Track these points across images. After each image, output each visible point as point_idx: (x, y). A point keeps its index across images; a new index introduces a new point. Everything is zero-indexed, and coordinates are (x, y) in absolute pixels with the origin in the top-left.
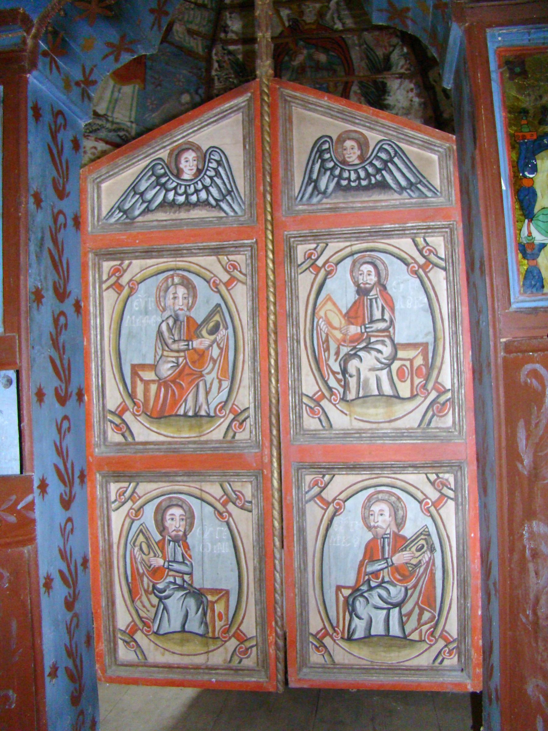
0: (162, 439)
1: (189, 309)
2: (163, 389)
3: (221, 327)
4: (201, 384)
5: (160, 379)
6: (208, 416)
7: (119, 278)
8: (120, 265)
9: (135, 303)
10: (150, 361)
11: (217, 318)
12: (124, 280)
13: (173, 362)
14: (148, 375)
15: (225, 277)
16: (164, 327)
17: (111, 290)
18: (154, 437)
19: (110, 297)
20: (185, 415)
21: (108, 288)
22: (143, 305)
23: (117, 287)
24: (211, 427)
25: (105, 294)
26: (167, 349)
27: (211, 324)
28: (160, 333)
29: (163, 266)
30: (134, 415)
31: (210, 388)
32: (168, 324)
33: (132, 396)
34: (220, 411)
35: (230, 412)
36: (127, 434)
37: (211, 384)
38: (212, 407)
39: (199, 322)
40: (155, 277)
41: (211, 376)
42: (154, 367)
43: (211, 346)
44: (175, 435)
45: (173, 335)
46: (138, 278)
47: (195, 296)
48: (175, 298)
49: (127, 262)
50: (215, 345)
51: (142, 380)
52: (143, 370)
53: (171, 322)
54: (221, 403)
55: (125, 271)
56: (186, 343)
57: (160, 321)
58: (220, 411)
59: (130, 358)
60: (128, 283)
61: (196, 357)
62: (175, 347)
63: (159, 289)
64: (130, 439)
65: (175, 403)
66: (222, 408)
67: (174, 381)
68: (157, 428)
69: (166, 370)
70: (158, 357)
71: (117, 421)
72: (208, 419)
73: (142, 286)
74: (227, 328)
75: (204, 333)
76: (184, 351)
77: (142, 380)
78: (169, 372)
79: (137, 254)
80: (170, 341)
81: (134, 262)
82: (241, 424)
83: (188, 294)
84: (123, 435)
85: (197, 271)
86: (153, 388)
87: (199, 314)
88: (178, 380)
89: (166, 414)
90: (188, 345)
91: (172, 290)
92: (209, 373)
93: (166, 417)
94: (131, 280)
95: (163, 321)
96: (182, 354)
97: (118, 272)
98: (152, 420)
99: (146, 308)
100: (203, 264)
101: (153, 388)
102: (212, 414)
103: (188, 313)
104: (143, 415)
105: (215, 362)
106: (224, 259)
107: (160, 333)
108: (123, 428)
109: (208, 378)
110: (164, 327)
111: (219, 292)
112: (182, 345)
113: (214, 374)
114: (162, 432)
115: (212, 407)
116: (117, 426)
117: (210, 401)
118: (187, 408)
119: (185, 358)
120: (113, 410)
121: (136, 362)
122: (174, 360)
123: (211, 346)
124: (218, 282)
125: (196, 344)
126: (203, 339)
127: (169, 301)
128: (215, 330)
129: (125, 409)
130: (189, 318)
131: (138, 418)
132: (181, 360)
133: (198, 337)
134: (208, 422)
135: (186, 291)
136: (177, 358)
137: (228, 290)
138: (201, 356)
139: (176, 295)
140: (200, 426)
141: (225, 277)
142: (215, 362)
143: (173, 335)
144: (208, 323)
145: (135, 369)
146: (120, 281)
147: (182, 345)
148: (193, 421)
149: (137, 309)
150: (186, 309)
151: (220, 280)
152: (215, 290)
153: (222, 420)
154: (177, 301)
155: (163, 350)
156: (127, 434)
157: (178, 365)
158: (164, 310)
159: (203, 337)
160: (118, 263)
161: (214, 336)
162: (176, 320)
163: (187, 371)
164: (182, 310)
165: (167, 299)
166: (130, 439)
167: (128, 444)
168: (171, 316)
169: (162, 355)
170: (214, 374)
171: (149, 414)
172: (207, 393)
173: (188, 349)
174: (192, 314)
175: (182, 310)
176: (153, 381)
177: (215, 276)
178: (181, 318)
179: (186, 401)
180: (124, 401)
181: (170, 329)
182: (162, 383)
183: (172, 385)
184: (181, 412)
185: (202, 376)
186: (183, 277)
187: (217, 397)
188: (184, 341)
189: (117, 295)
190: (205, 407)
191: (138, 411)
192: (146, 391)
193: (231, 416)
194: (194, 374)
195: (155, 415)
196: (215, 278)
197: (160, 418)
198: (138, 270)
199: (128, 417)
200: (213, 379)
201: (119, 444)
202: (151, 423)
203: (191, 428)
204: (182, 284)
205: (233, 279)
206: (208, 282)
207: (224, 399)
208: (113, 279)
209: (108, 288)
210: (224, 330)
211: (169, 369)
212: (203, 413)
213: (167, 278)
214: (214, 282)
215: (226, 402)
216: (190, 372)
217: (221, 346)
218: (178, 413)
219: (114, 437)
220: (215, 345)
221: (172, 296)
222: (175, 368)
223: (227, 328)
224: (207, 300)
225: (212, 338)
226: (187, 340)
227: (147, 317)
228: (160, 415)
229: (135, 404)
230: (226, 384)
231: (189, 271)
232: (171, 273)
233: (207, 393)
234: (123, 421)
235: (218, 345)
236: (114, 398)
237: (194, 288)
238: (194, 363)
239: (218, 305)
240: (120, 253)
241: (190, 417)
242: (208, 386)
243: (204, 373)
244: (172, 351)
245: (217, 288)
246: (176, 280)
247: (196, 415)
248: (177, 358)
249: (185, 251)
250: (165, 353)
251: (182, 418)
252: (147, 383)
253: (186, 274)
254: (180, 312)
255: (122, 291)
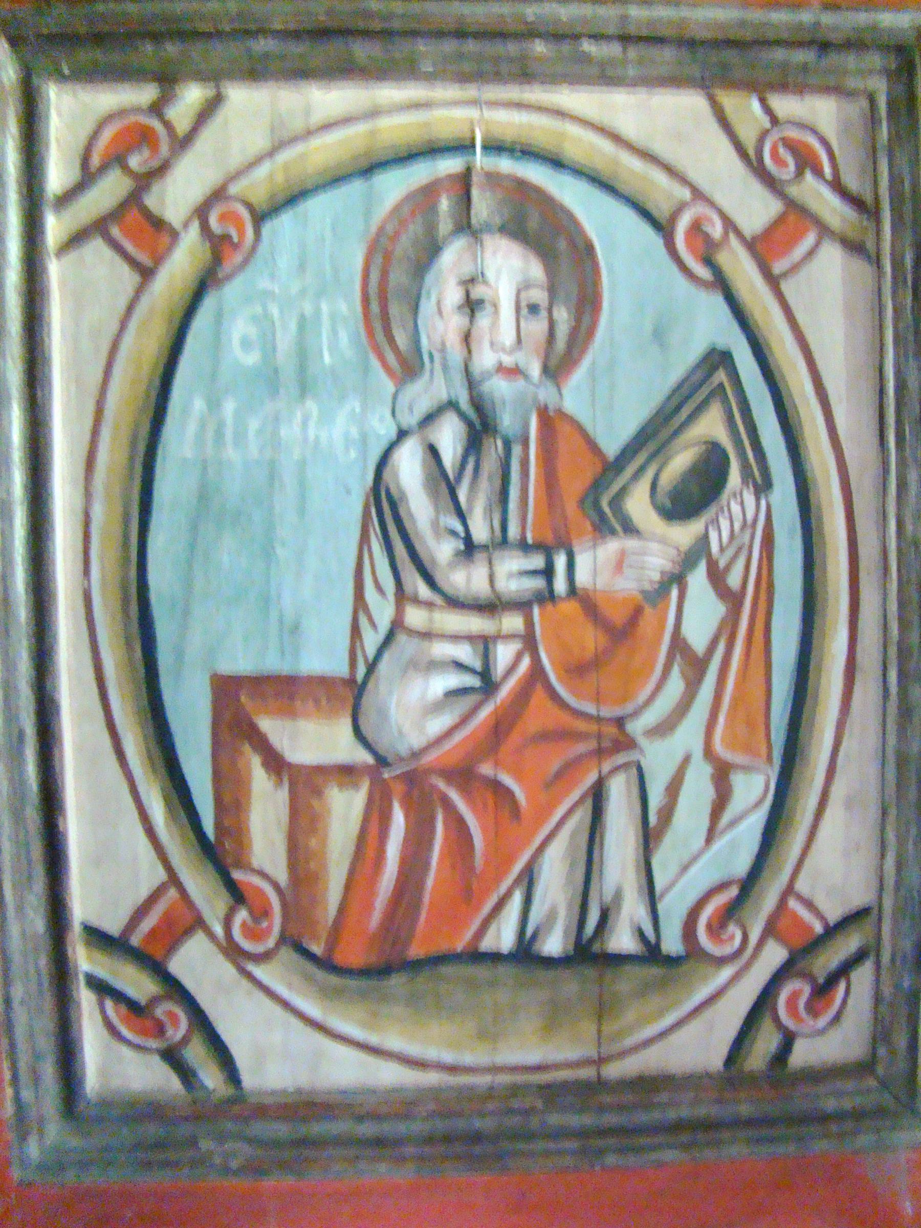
0: (389, 1075)
1: (557, 368)
2: (399, 818)
3: (734, 477)
4: (619, 791)
5: (382, 761)
6: (652, 953)
7: (145, 181)
8: (157, 109)
9: (240, 328)
10: (322, 654)
11: (711, 425)
12: (178, 194)
13: (459, 666)
14: (315, 739)
15: (756, 209)
16: (409, 467)
17: (96, 251)
18: (343, 1070)
19: (85, 290)
20: (525, 953)
21: (76, 240)
22: (285, 342)
23: (136, 231)
24: (661, 1013)
25: (54, 269)
26: (424, 591)
27: (680, 461)
28: (383, 502)
29: (397, 128)
30: (233, 952)
31: (667, 813)
32: (433, 451)
33: (220, 853)
34: (717, 928)
35: (770, 930)
36: (196, 1053)
37: (674, 789)
38: (674, 909)
39: (611, 447)
40: (357, 187)
41: (673, 746)
42: (350, 693)
43: (677, 578)
44: (468, 1059)
45: (461, 516)
46: (258, 185)
47: (588, 303)
48: (471, 306)
49: (192, 95)
50: (698, 579)
51: (275, 763)
52: (290, 713)
53: (449, 437)
54: (722, 887)
55: (183, 143)
56: (537, 561)
57: (385, 430)
58: (717, 928)
59: (206, 645)
60: (202, 212)
61: (590, 639)
62: (470, 580)
63: (379, 250)
64: (211, 1078)
65: (468, 888)
66: (730, 912)
67: (463, 775)
68: (364, 1025)
69: (417, 708)
70: (371, 641)
71: (138, 984)
72: (655, 971)
73: (283, 226)
74: (763, 486)
75: (639, 505)
76: (522, 606)
77: (275, 763)
78: (437, 725)
79: (262, 45)
80: (443, 551)
81: (239, 95)
82: (823, 990)
83: (552, 290)
84: (172, 1057)
85: (600, 165)
86: (345, 808)
87: (611, 398)
88: (486, 769)
89: (416, 951)
90: (548, 572)
91: (453, 258)
92: (665, 728)
93: (415, 966)
94: (218, 195)
95: (402, 434)
96: (513, 622)
97: (140, 151)
98: (334, 980)
99: (303, 355)
100: (629, 128)
101: (345, 808)
102: (672, 944)
103: (547, 394)
104: (287, 954)
105: (696, 667)
106: (748, 112)
107: (383, 502)
108: (174, 1020)
109: (659, 759)
110: (409, 467)
111: (721, 284)
112: (512, 573)
113: (689, 735)
114: (394, 1042)
115: (674, 909)
116: (134, 1008)
117: (660, 883)
118: (536, 915)
119: (529, 641)
120: (113, 925)
121: (240, 662)
122: (464, 653)
123: (677, 578)
124: (716, 230)
125: (592, 564)
126: (631, 543)
127: (440, 322)
128: (693, 497)
129: (183, 923)
130: (550, 420)
131: (259, 971)
132: (504, 654)
133: (602, 528)
134: (644, 990)
135: (537, 271)
136: (485, 643)
137: (773, 281)
138: (620, 629)
139: (478, 292)
140: (603, 1010)
141: (756, 209)
142: (696, 667)
143: (461, 516)
144: (661, 453)
145: (239, 704)
146: (151, 201)
147: (512, 573)
148: (570, 985)
149: (251, 359)
150: (535, 370)
151: (729, 224)
152: (703, 272)
153: (726, 973)
154: (483, 321)
155: (402, 596)
156: (196, 1053)
157: (489, 685)
158: (409, 367)
159: (629, 529)
160: (146, 94)
161: (695, 527)
162: (480, 427)
163: (539, 715)
164: (514, 372)
165: (427, 307)
166: (211, 1078)
167: (203, 1112)
168: (452, 405)
169: (397, 625)
170: (689, 735)
171: (317, 949)
172: (649, 838)
173: (547, 597)
174: (574, 397)
175: (514, 372)
176: (346, 773)
177: (698, 194)
178: (507, 421)
179: (528, 878)
180: (173, 879)
181: (443, 484)
182: (396, 781)
183: (454, 796)
184: (503, 936)
185: (626, 743)
186: (523, 189)
187: (700, 860)
188: (524, 547)
189: (128, 278)
190: (633, 909)
191: (251, 933)
192: (303, 824)
193: (774, 955)
194: (579, 736)
195: (353, 954)
196: (699, 209)
197: (383, 971)
198: (259, 142)
199: (197, 963)
200: (687, 760)
201: (145, 1110)
202: (327, 994)
203: (554, 1020)
204: (516, 229)
205: (795, 217)
206: (663, 228)
207: (742, 865)
208: (110, 190)
209: (76, 240)
210: (749, 498)
211: (437, 707)
212: (622, 940)
213: (428, 194)
214: (696, 227)
215: (749, 883)
216: (554, 726)
217: (734, 580)
218: (487, 944)
219: (112, 1063)
220: (698, 579)
221: (453, 296)
222: (464, 704)
223: (763, 486)
224: (652, 326)
225: (684, 534)
226: (542, 547)
227: (311, 405)
228: (380, 961)
229: (237, 894)
230: (752, 788)
231: (557, 163)
232: (450, 165)
233: (649, 838)
234: (176, 989)
235: (716, 577)
236: (113, 861)
237: (584, 253)
238: (578, 670)
239: (718, 359)
240: (156, 37)
241: (549, 962)
242: (656, 800)
243: (636, 727)
244: (454, 603)
245: (708, 262)
246: (483, 206)
247: (587, 953)
248: (485, 643)
249: (539, 47)
250: (415, 617)
251: (504, 971)
252: (305, 786)
253: (536, 174)
254: (500, 389)
255: (159, 259)
